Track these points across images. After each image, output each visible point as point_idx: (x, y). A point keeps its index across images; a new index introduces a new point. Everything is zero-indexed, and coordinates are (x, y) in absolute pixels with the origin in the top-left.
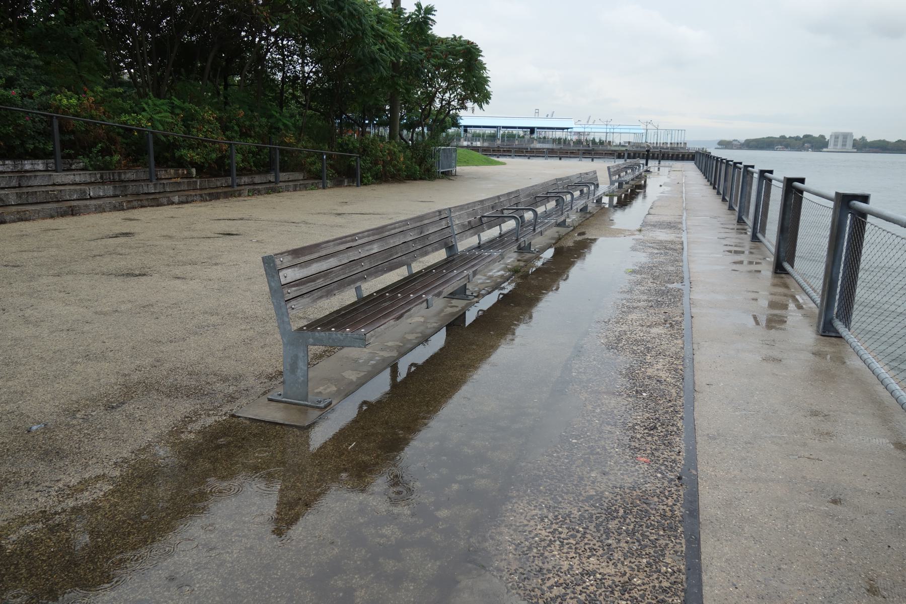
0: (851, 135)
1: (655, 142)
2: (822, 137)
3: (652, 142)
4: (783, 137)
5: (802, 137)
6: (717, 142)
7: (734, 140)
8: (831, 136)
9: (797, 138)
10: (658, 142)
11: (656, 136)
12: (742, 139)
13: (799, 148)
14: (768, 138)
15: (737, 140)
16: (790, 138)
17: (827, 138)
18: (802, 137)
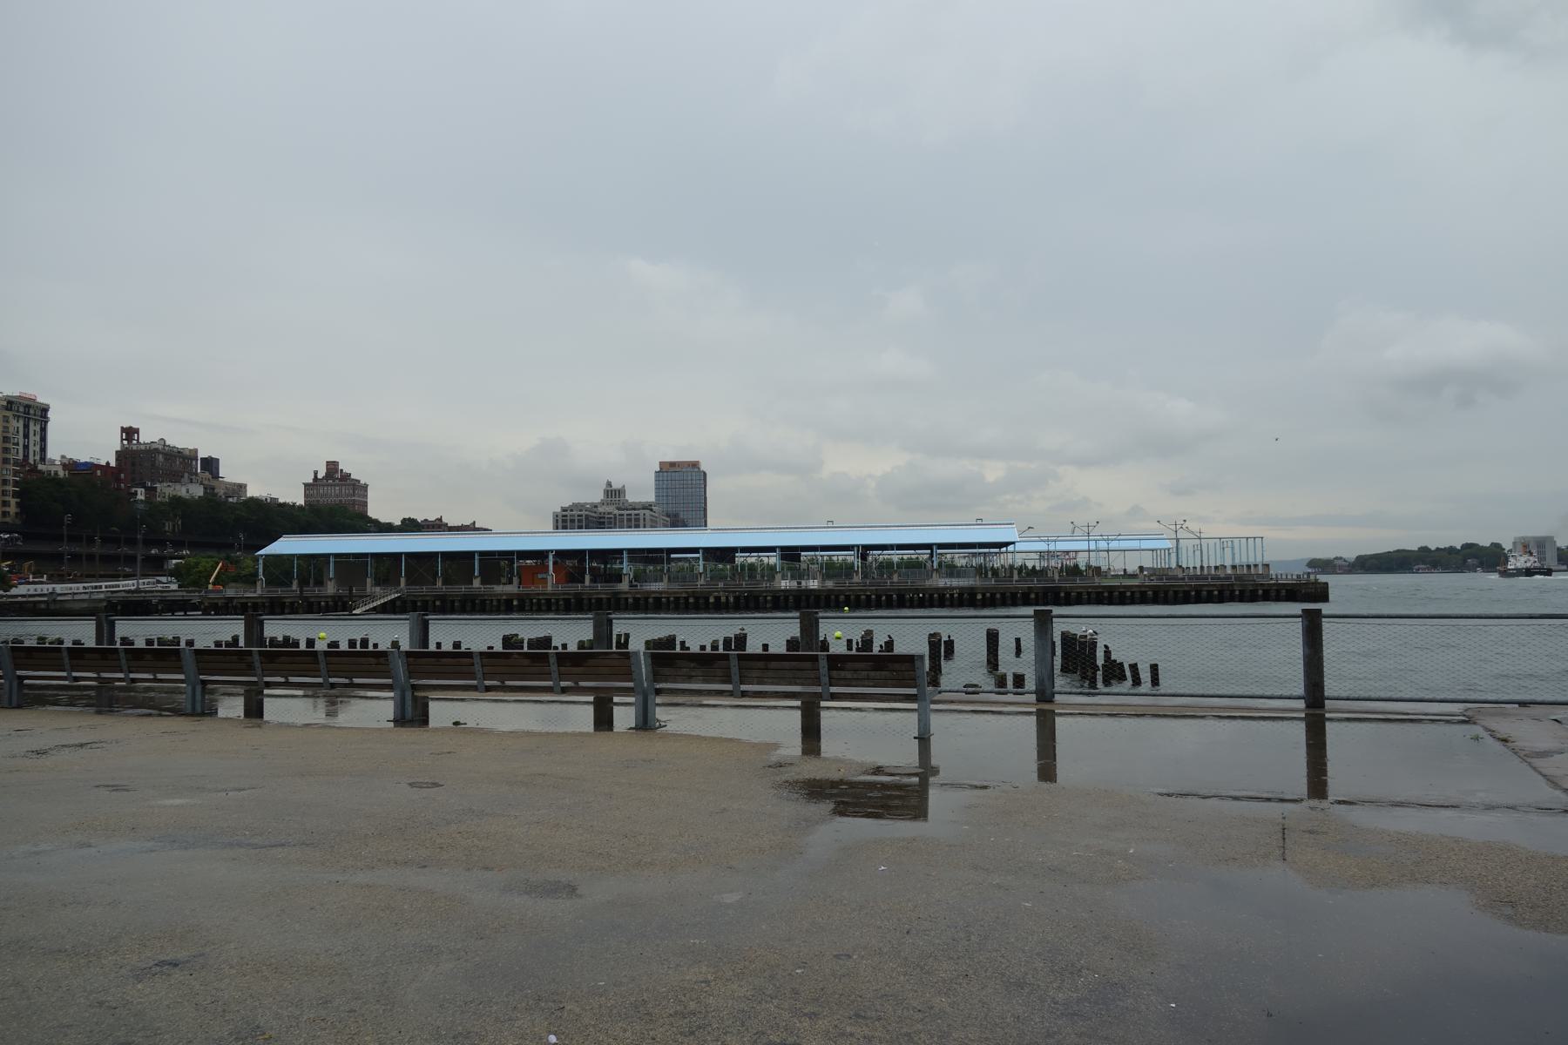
0: (1551, 540)
1: (1198, 566)
2: (1497, 546)
3: (1191, 566)
4: (1424, 549)
5: (1459, 548)
6: (1307, 561)
7: (1336, 558)
8: (1514, 543)
9: (1451, 550)
10: (1205, 565)
11: (1198, 553)
12: (1351, 555)
13: (1459, 568)
14: (1398, 551)
15: (1341, 558)
16: (1438, 549)
17: (1507, 546)
18: (1459, 548)
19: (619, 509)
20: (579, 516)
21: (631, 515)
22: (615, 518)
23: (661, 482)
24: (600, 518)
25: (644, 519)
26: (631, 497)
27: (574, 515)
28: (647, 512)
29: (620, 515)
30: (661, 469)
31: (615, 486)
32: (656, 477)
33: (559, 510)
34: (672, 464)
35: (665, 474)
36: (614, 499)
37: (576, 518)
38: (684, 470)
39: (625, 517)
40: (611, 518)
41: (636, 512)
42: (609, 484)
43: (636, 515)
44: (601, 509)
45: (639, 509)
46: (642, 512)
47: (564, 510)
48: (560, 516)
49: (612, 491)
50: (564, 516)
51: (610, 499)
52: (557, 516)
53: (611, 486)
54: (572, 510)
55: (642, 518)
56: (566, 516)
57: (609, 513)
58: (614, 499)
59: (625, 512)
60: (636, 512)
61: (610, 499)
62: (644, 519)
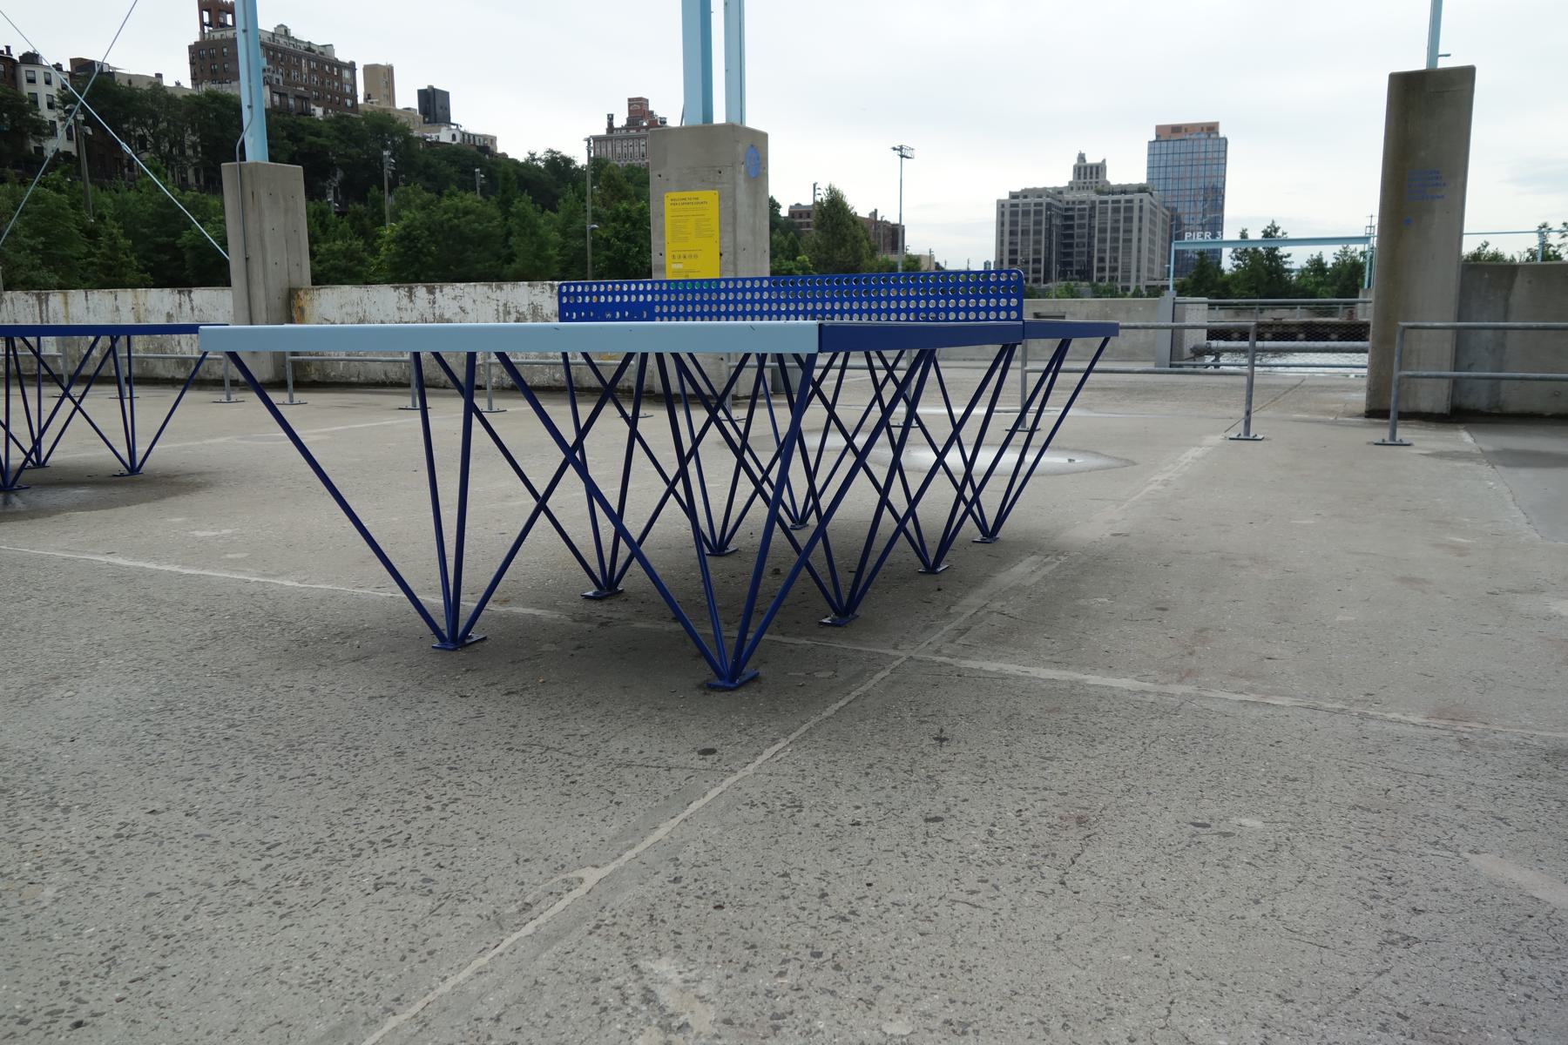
19: (1100, 192)
20: (1036, 205)
21: (1119, 202)
22: (1093, 208)
23: (1157, 158)
24: (1067, 210)
25: (1141, 209)
26: (1114, 177)
27: (1029, 204)
28: (1145, 196)
29: (1101, 202)
30: (1157, 136)
31: (1091, 159)
32: (1150, 148)
33: (1006, 197)
34: (1176, 129)
35: (1164, 144)
36: (1088, 180)
37: (1032, 209)
38: (1194, 136)
39: (1110, 206)
40: (1084, 209)
41: (1128, 197)
42: (1082, 157)
43: (1128, 201)
44: (1068, 197)
45: (1132, 192)
46: (1137, 196)
47: (1014, 196)
48: (1007, 206)
49: (1085, 168)
50: (1013, 205)
51: (1082, 180)
52: (1003, 206)
53: (1085, 161)
54: (1025, 197)
55: (1136, 205)
56: (1016, 205)
57: (1082, 202)
58: (1088, 180)
59: (1110, 198)
60: (1128, 197)
61: (1082, 180)
62: (1141, 209)
